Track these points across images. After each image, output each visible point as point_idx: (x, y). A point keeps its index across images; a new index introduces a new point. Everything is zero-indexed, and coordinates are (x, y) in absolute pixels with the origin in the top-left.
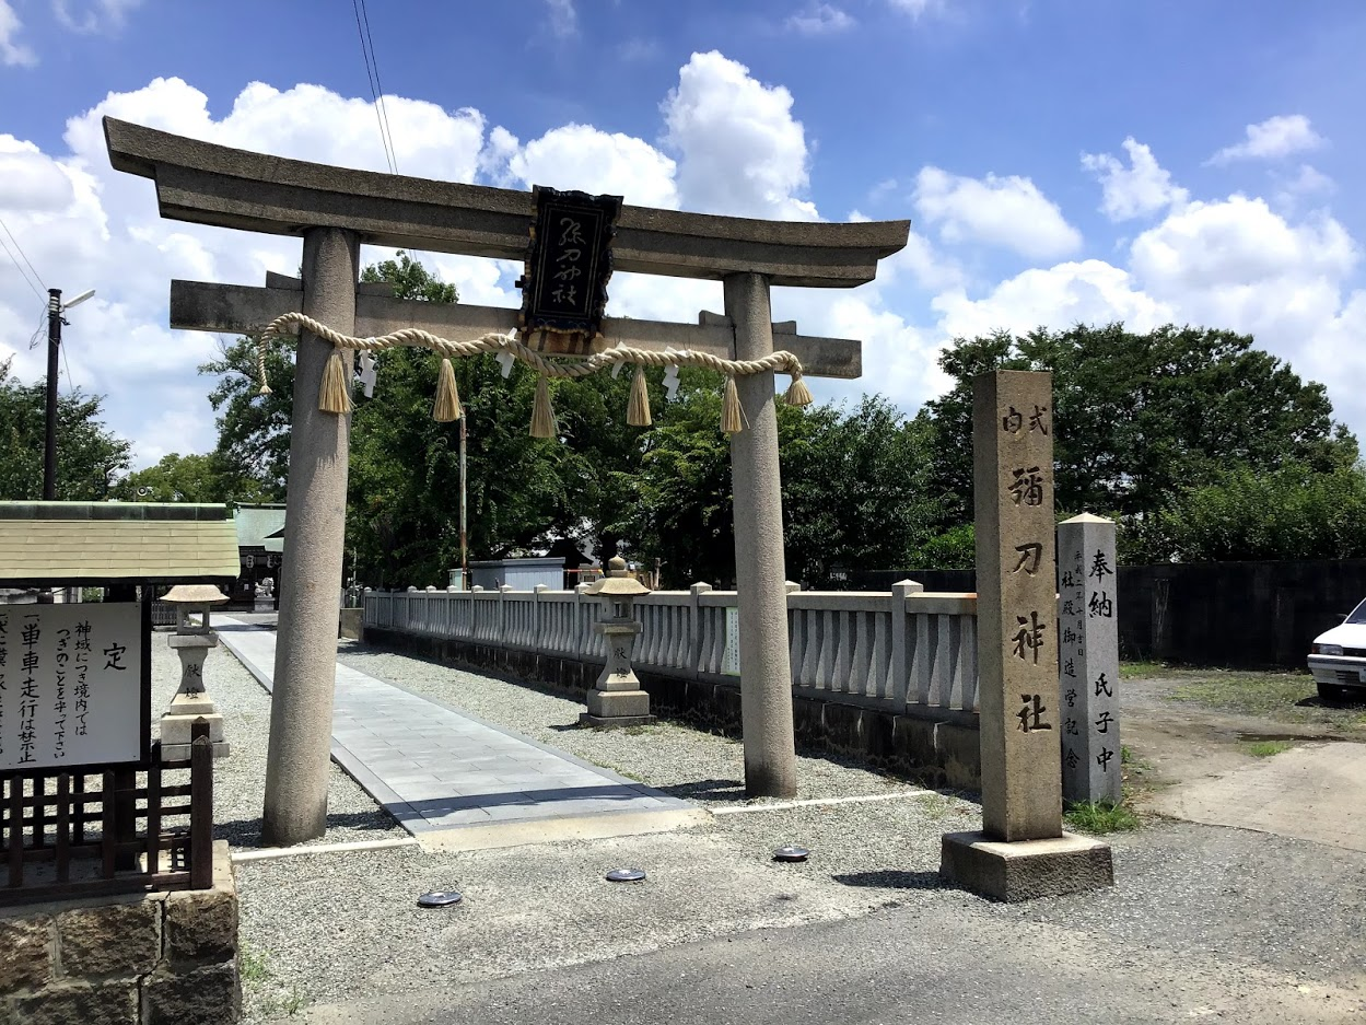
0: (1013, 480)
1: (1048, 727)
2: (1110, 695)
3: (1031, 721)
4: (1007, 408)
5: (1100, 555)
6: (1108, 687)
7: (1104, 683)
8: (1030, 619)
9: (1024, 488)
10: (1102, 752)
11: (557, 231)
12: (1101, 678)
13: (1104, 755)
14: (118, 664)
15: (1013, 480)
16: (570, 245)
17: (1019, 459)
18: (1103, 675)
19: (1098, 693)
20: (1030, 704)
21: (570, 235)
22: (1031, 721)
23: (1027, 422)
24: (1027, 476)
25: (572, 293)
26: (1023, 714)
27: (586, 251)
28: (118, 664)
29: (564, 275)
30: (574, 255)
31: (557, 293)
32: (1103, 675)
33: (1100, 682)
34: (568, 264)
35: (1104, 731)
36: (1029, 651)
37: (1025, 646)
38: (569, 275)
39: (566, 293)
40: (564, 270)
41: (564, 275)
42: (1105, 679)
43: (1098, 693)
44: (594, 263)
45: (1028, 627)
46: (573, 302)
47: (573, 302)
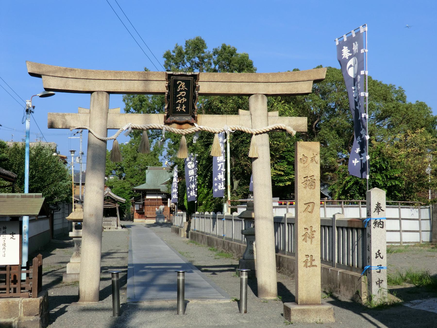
0: (303, 180)
1: (316, 266)
2: (382, 258)
3: (309, 264)
4: (302, 155)
5: (378, 204)
6: (381, 255)
7: (379, 254)
8: (309, 229)
9: (308, 183)
10: (378, 280)
11: (176, 86)
12: (378, 252)
13: (379, 281)
14: (13, 238)
15: (303, 180)
16: (181, 91)
17: (306, 173)
18: (379, 250)
19: (376, 257)
20: (309, 259)
21: (181, 87)
22: (309, 264)
23: (309, 160)
24: (309, 178)
25: (184, 107)
26: (306, 262)
27: (188, 92)
28: (13, 238)
29: (180, 101)
30: (183, 94)
31: (178, 108)
32: (379, 250)
33: (378, 253)
34: (182, 97)
35: (379, 272)
36: (309, 240)
37: (307, 238)
38: (182, 101)
39: (181, 107)
40: (180, 99)
41: (180, 101)
42: (380, 252)
43: (376, 257)
44: (191, 98)
45: (309, 231)
46: (185, 111)
47: (185, 111)
